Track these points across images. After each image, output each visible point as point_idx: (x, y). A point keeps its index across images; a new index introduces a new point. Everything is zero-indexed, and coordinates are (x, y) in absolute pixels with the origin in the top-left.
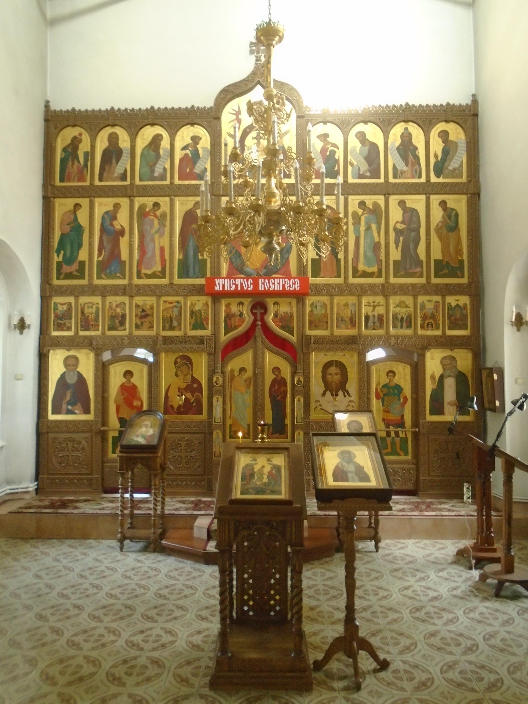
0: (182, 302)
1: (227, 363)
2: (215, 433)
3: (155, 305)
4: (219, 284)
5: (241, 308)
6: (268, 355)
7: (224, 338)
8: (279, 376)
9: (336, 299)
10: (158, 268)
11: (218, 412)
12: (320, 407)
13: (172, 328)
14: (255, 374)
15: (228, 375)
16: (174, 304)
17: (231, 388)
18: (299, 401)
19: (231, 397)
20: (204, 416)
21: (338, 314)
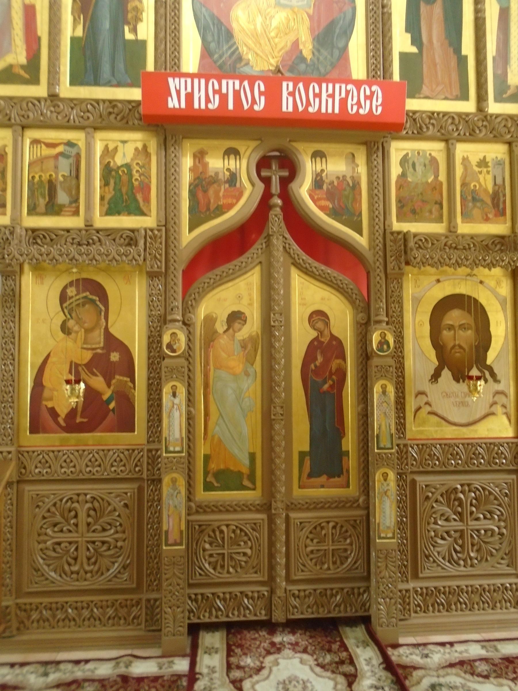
0: (82, 144)
1: (197, 301)
2: (166, 480)
3: (9, 150)
4: (178, 92)
5: (232, 164)
6: (297, 279)
7: (189, 237)
8: (326, 332)
9: (462, 149)
10: (18, 56)
11: (174, 425)
12: (428, 409)
13: (53, 209)
14: (267, 327)
15: (198, 330)
16: (60, 149)
17: (207, 363)
18: (384, 392)
19: (206, 386)
20: (139, 435)
21: (464, 185)
